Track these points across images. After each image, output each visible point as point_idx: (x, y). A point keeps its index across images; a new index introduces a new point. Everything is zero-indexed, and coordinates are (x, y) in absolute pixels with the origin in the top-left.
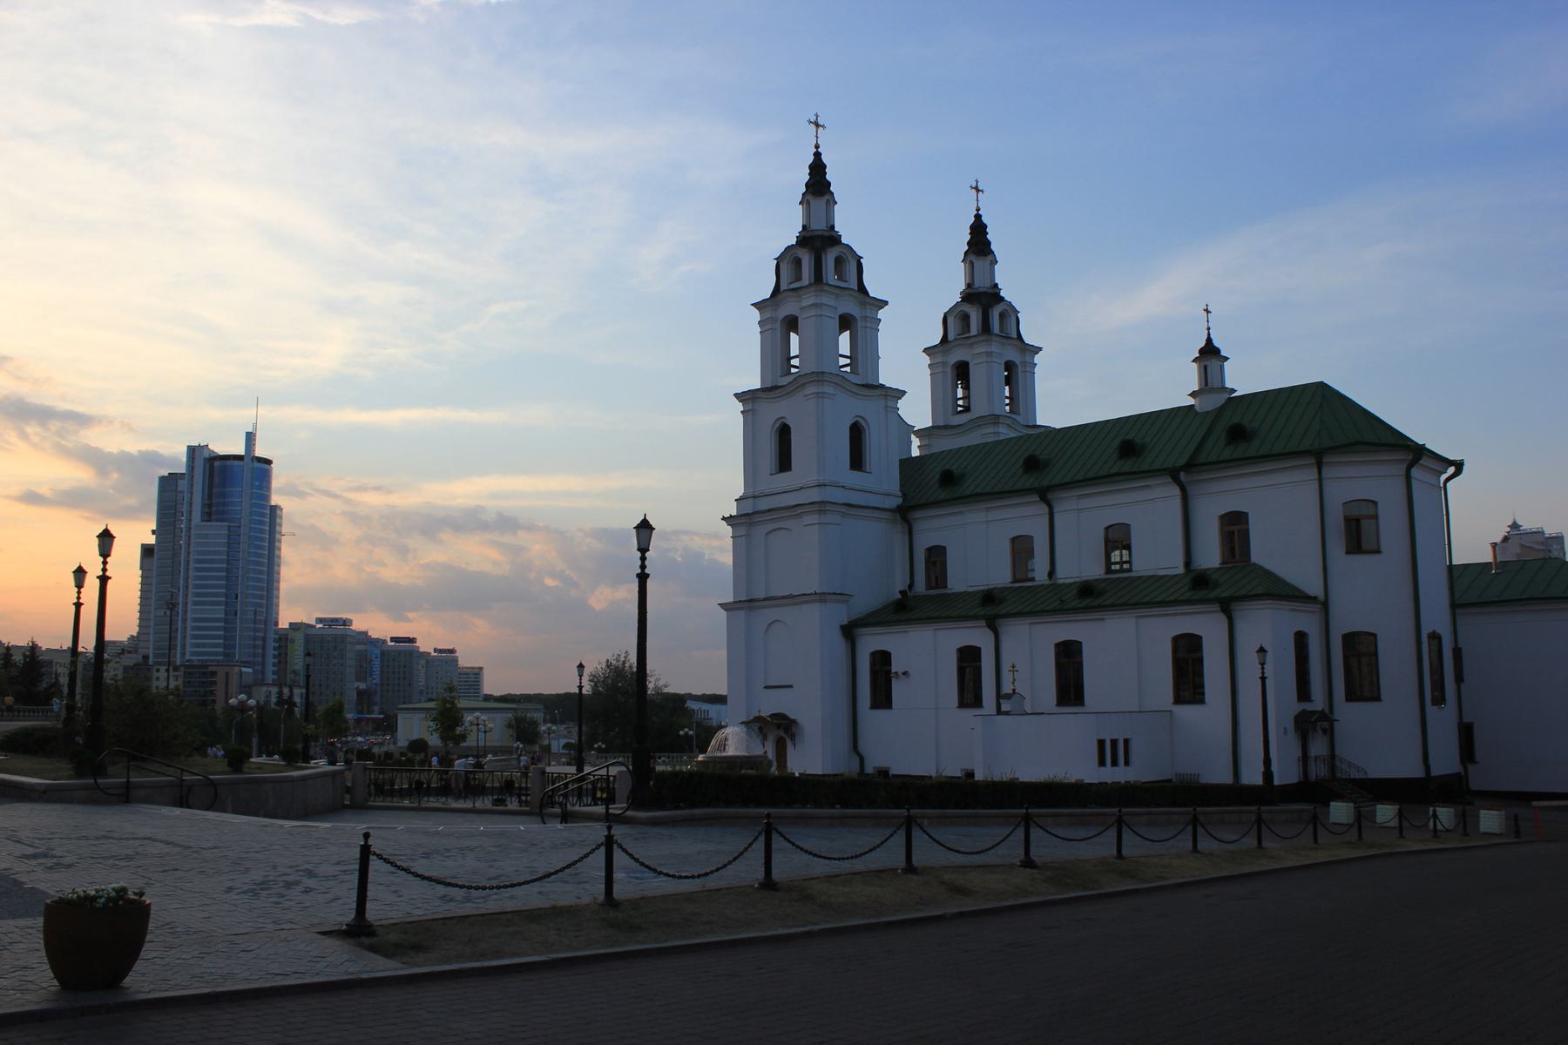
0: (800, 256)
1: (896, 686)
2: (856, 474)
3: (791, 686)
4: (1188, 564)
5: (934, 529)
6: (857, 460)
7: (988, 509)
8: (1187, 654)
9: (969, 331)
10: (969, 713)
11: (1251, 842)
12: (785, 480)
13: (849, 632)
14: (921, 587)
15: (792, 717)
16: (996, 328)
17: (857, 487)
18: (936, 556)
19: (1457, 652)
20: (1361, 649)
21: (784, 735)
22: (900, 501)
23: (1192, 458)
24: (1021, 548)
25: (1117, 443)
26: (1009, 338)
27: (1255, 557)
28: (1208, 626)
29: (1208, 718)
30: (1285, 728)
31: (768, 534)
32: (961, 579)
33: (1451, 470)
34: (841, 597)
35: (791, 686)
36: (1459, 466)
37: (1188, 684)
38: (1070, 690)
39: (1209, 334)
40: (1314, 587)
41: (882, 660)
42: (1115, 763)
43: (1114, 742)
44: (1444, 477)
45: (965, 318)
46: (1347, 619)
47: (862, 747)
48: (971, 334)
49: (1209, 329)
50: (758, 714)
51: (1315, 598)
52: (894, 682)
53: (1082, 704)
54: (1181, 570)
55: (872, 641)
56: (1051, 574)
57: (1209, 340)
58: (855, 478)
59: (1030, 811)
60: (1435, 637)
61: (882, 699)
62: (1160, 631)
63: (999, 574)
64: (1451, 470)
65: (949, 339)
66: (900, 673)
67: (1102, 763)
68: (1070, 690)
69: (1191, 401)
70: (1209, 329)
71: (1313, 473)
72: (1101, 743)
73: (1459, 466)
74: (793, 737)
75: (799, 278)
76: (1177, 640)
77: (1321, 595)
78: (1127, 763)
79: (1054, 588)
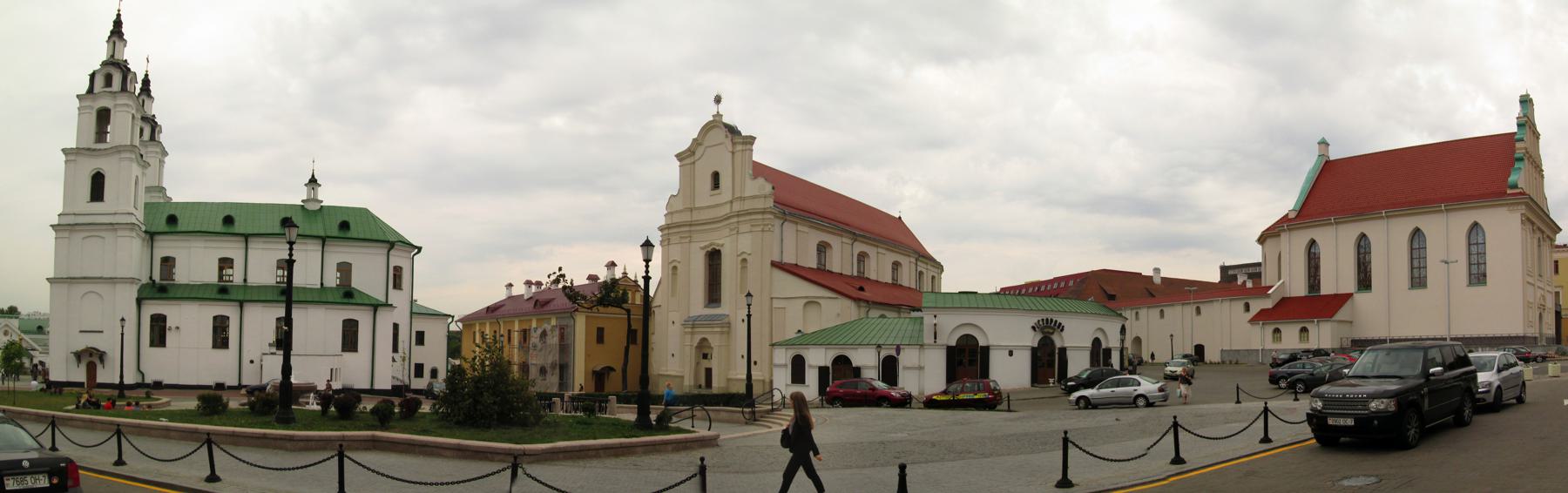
1: (170, 337)
3: (102, 332)
4: (322, 284)
5: (165, 248)
7: (207, 240)
10: (221, 352)
12: (97, 207)
13: (139, 302)
14: (157, 277)
15: (102, 350)
18: (168, 262)
24: (226, 263)
29: (361, 357)
31: (84, 238)
32: (182, 275)
33: (416, 250)
35: (102, 332)
36: (420, 249)
37: (350, 341)
44: (412, 254)
47: (141, 369)
52: (168, 332)
54: (319, 286)
55: (151, 308)
56: (245, 280)
61: (159, 338)
63: (211, 277)
64: (416, 250)
66: (173, 327)
71: (386, 251)
73: (420, 249)
79: (245, 286)
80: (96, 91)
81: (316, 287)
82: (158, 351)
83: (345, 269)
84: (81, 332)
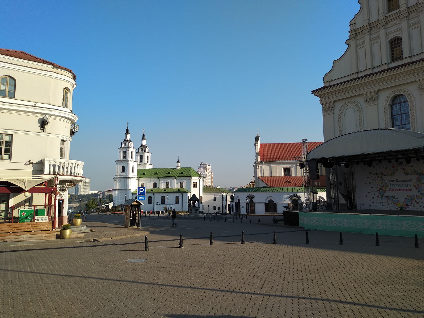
4: (176, 188)
8: (177, 198)
12: (123, 174)
16: (146, 152)
19: (203, 197)
21: (123, 208)
22: (137, 176)
24: (155, 185)
28: (179, 195)
37: (177, 202)
43: (170, 208)
57: (178, 161)
60: (201, 196)
62: (174, 196)
69: (176, 167)
80: (123, 147)
81: (174, 188)
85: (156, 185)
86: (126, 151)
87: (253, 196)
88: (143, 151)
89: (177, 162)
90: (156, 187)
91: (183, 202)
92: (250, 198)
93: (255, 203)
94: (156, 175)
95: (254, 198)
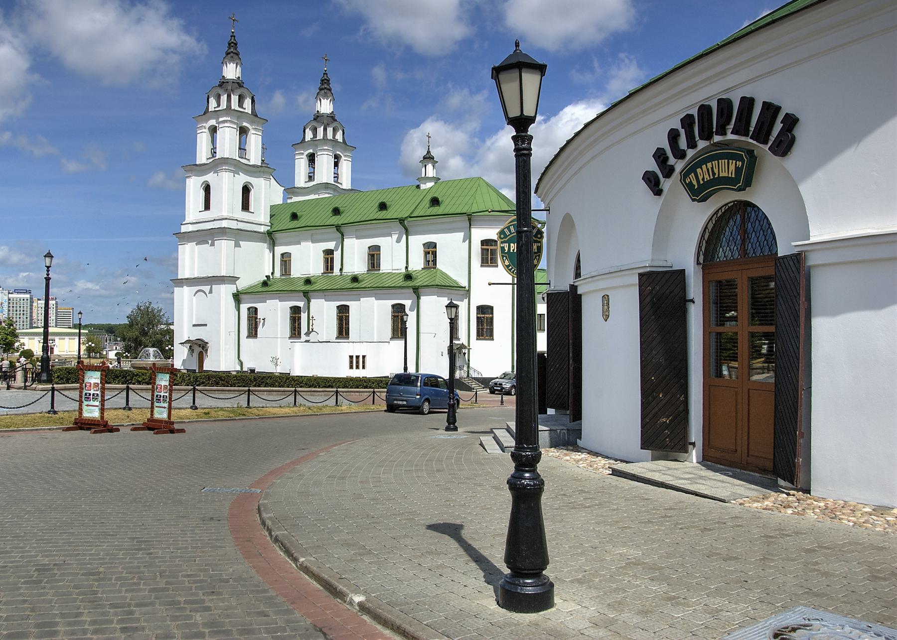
0: (220, 93)
2: (245, 213)
3: (206, 325)
6: (245, 206)
8: (399, 312)
9: (316, 137)
11: (332, 401)
12: (207, 215)
13: (237, 297)
14: (277, 274)
17: (245, 220)
18: (286, 260)
20: (485, 314)
23: (411, 213)
25: (377, 204)
26: (336, 141)
27: (439, 266)
30: (442, 352)
32: (298, 271)
34: (233, 279)
35: (206, 325)
38: (343, 331)
39: (429, 149)
40: (464, 283)
41: (253, 312)
42: (357, 367)
43: (358, 357)
45: (315, 131)
46: (478, 299)
47: (241, 358)
48: (317, 139)
49: (429, 146)
50: (188, 339)
51: (465, 287)
53: (348, 338)
56: (341, 270)
57: (429, 152)
58: (245, 216)
59: (250, 388)
61: (253, 332)
65: (306, 140)
67: (351, 367)
68: (343, 331)
70: (429, 146)
72: (351, 357)
74: (207, 350)
75: (219, 105)
76: (393, 306)
77: (467, 288)
78: (364, 367)
81: (400, 271)
82: (252, 341)
83: (431, 250)
84: (194, 325)
85: (332, 259)
86: (219, 123)
87: (770, 110)
88: (320, 135)
89: (425, 158)
90: (332, 269)
91: (422, 330)
92: (704, 173)
93: (813, 260)
94: (336, 220)
95: (784, 147)
